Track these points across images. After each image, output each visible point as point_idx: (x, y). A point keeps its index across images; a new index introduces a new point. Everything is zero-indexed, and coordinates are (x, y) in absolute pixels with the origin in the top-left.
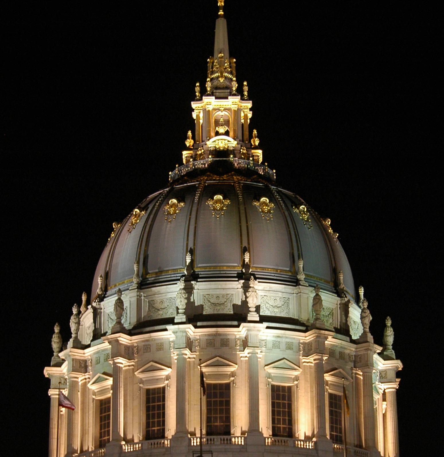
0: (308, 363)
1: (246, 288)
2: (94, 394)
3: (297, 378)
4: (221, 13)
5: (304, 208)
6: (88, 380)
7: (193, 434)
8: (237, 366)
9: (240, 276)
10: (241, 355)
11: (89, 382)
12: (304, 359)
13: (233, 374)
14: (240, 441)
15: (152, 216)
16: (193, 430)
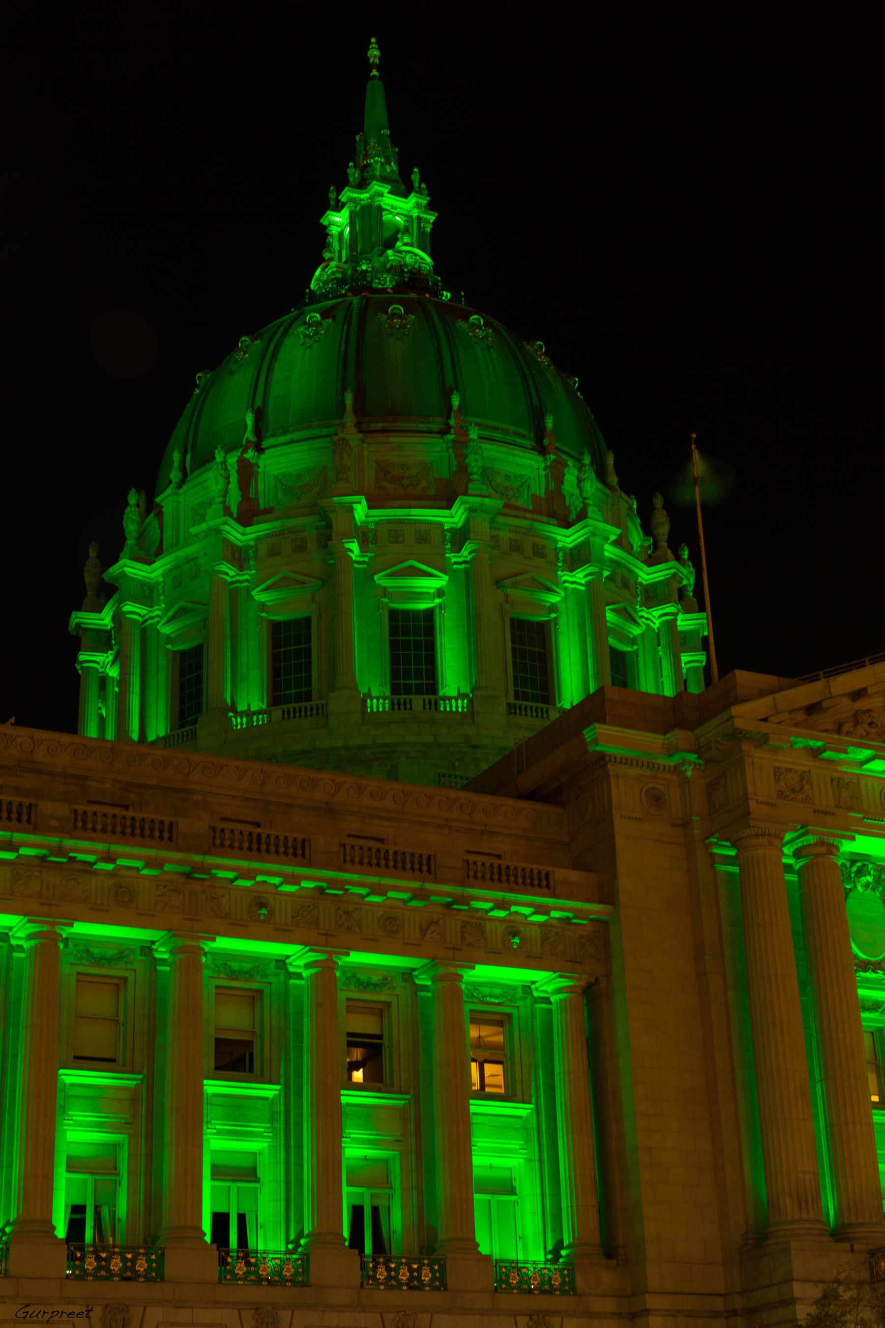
0: (572, 583)
1: (460, 446)
2: (169, 640)
3: (553, 608)
4: (375, 73)
5: (541, 347)
6: (156, 619)
7: (368, 695)
8: (446, 578)
9: (443, 432)
10: (453, 560)
11: (158, 622)
12: (566, 576)
13: (440, 593)
14: (460, 706)
15: (274, 343)
16: (366, 691)
